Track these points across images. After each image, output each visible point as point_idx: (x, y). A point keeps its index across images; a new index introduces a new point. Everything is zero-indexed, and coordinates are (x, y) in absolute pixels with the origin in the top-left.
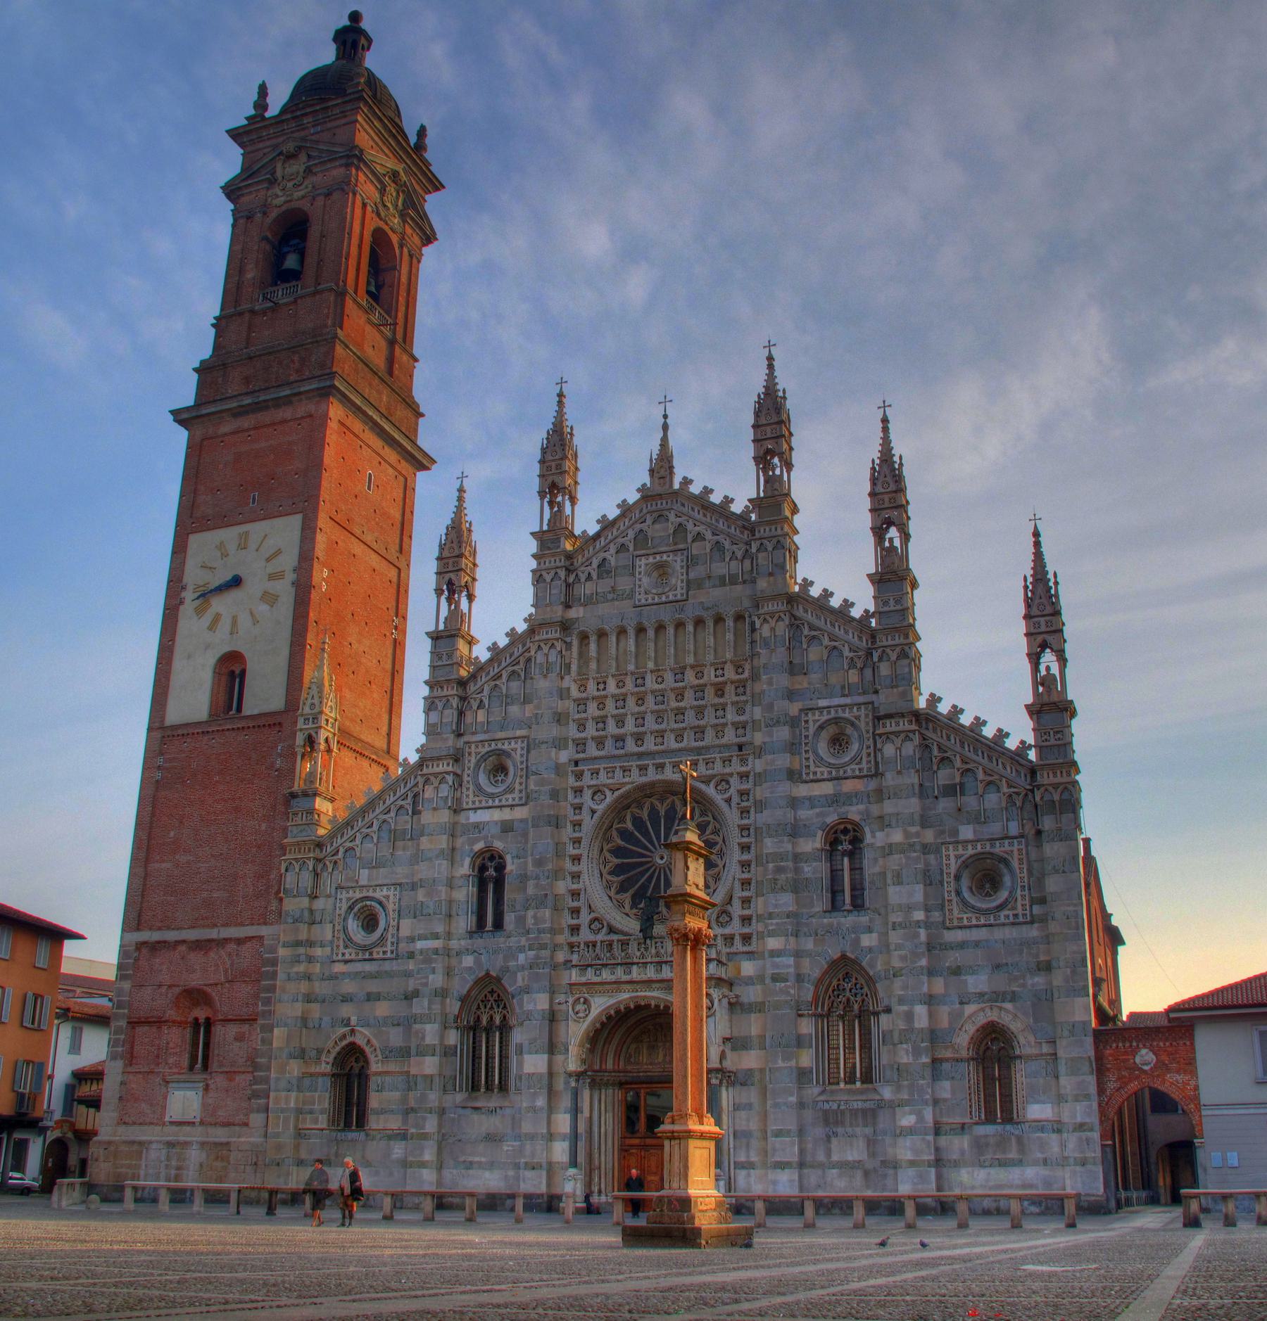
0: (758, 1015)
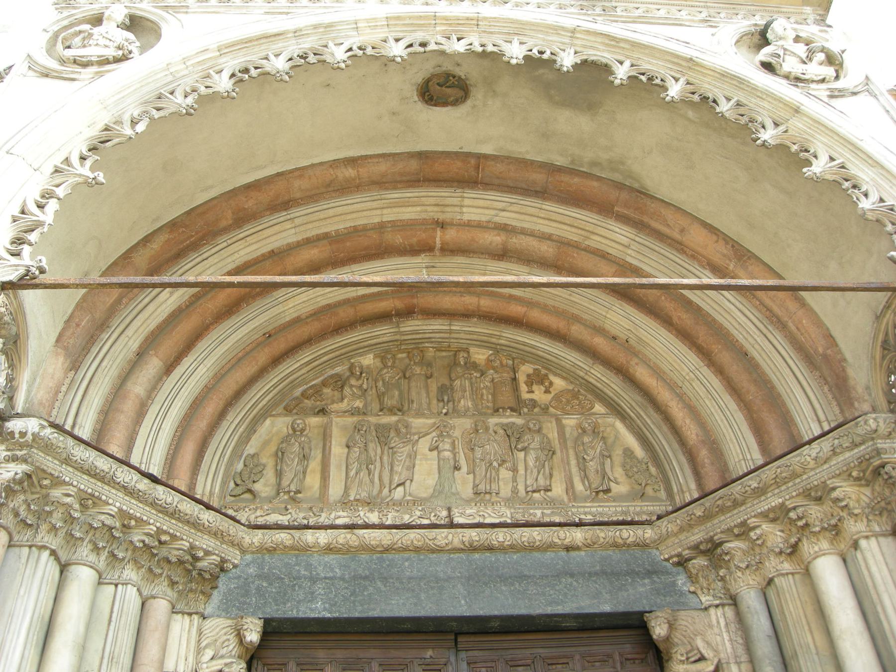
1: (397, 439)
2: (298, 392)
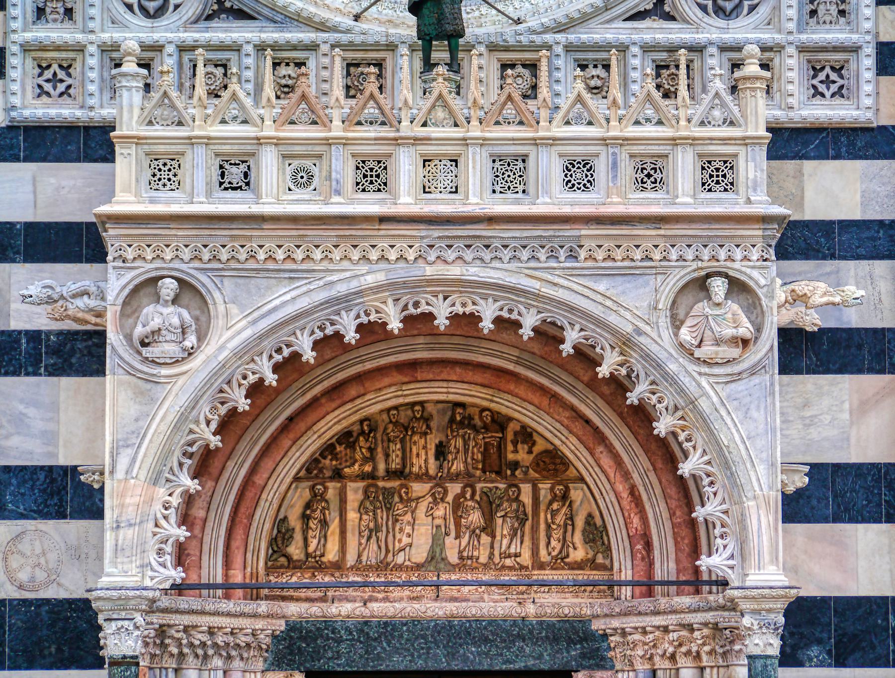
1: (401, 506)
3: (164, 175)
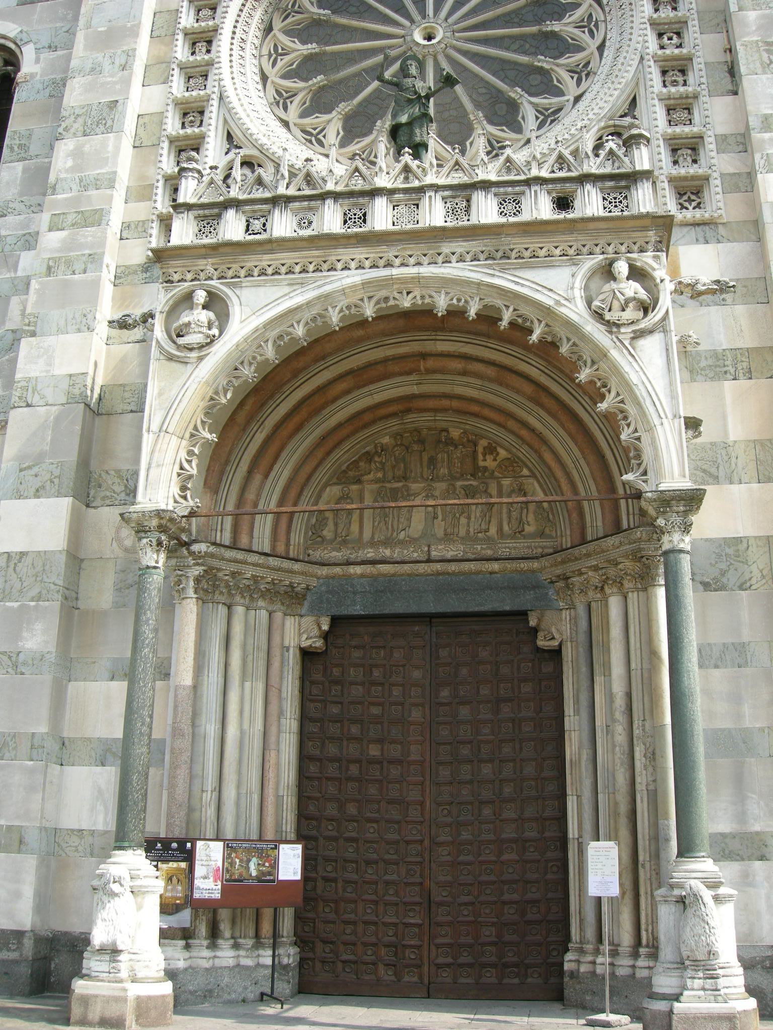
0: (743, 383)
2: (344, 467)
3: (207, 229)
